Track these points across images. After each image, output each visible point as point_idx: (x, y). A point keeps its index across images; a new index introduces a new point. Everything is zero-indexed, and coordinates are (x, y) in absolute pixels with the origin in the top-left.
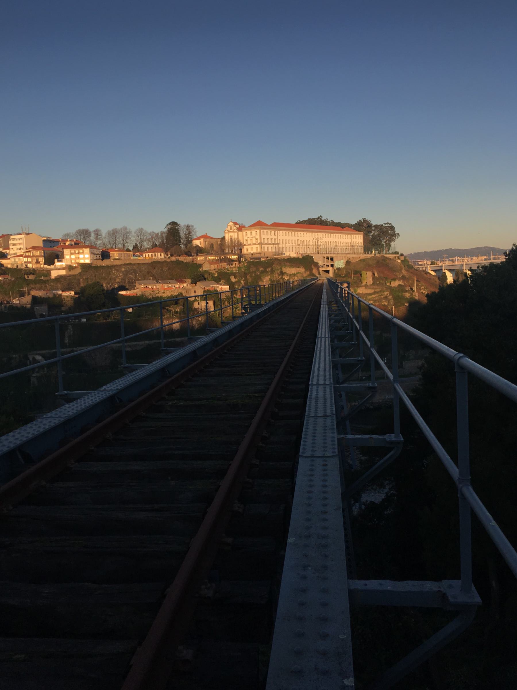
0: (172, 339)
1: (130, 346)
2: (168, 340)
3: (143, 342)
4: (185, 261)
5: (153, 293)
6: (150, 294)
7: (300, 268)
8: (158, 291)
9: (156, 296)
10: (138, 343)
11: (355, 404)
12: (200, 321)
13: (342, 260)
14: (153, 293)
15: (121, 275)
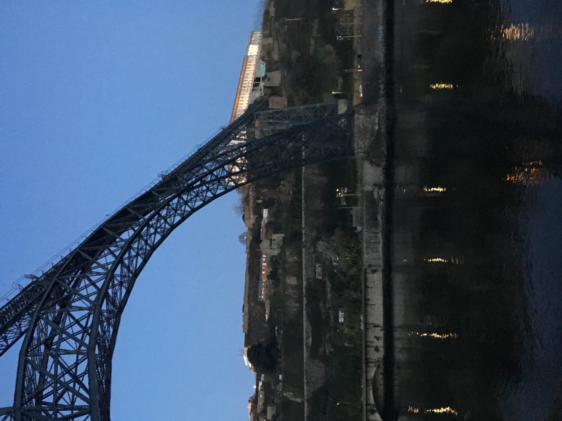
0: (304, 290)
1: (307, 338)
2: (304, 295)
3: (305, 323)
4: (251, 238)
5: (268, 288)
6: (269, 290)
7: (255, 124)
8: (267, 282)
9: (272, 285)
10: (305, 329)
11: (382, 89)
12: (290, 254)
13: (260, 66)
14: (268, 288)
15: (257, 307)
